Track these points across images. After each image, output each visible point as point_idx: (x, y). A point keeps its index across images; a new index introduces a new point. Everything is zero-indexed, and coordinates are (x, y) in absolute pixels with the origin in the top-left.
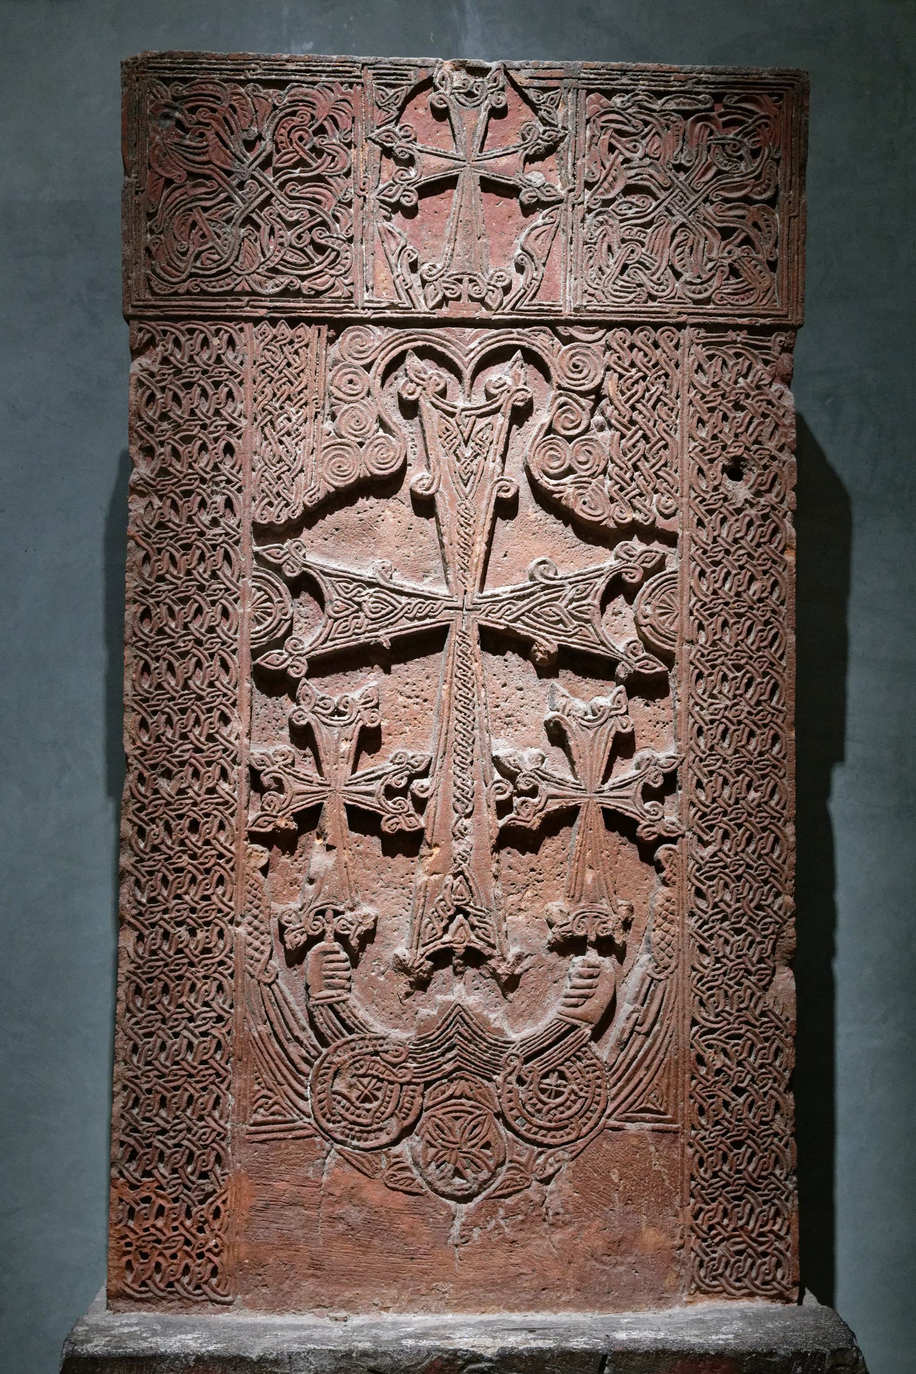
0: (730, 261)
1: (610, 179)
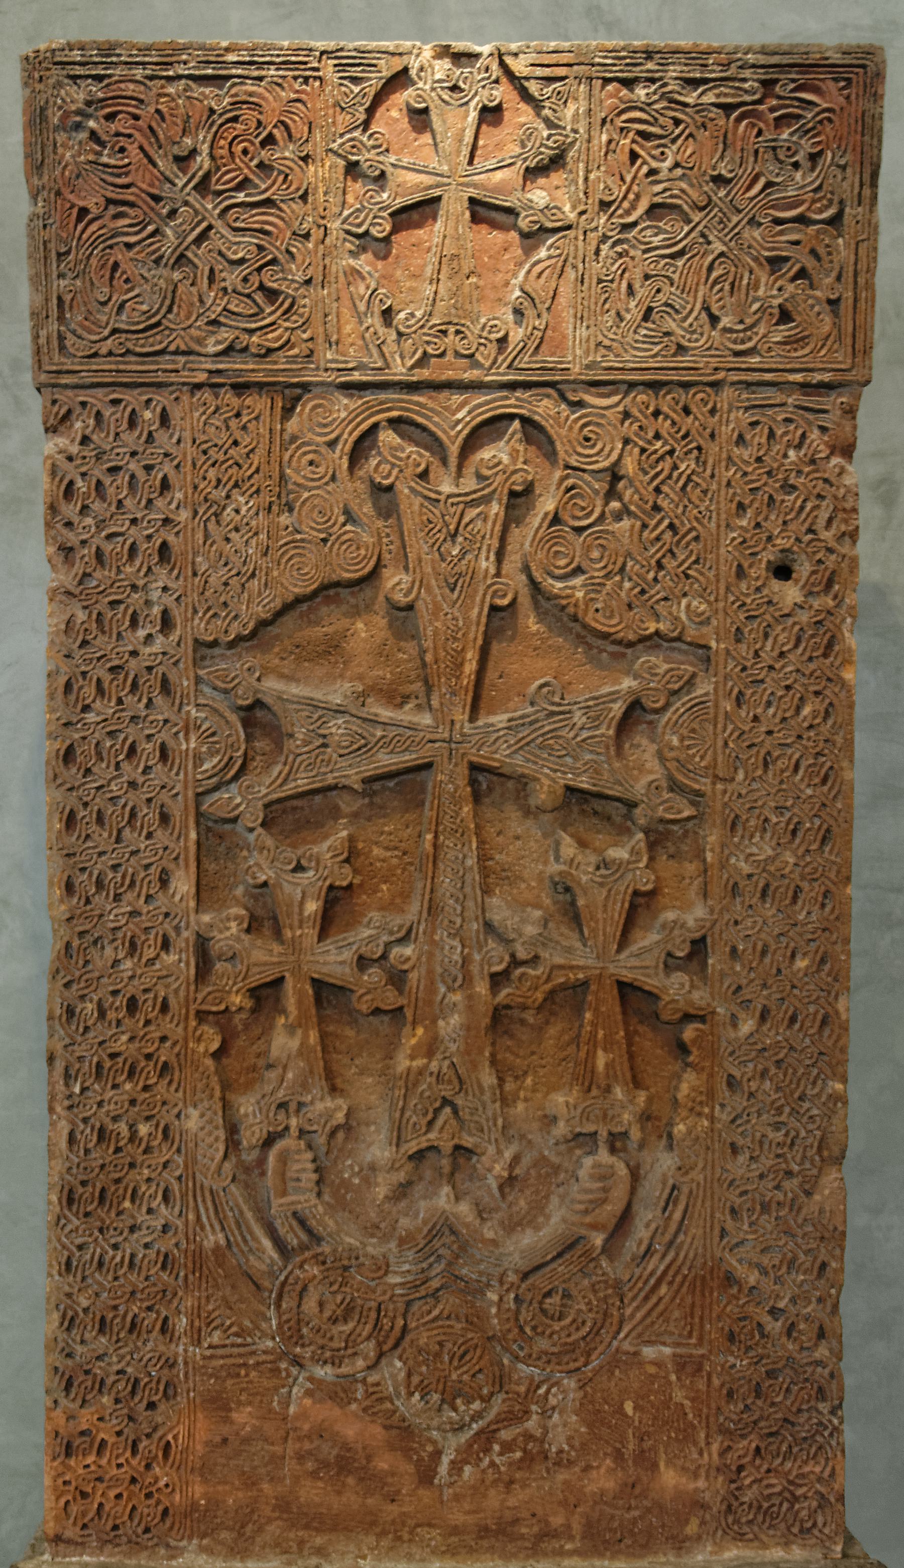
0: (780, 300)
1: (631, 196)
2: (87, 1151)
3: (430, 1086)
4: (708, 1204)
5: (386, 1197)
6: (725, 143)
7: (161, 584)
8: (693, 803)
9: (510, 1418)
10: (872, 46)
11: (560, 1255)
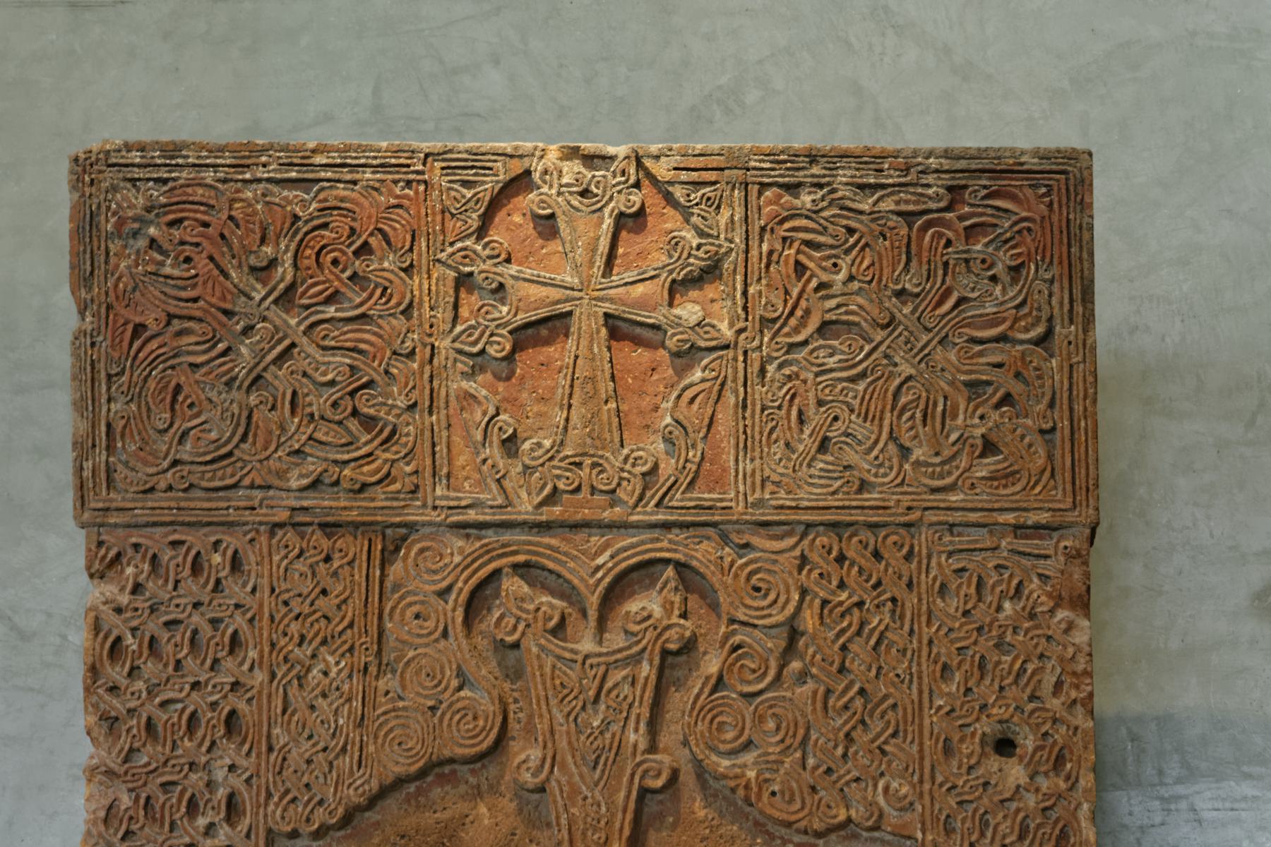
0: (983, 430)
1: (799, 313)
7: (228, 761)
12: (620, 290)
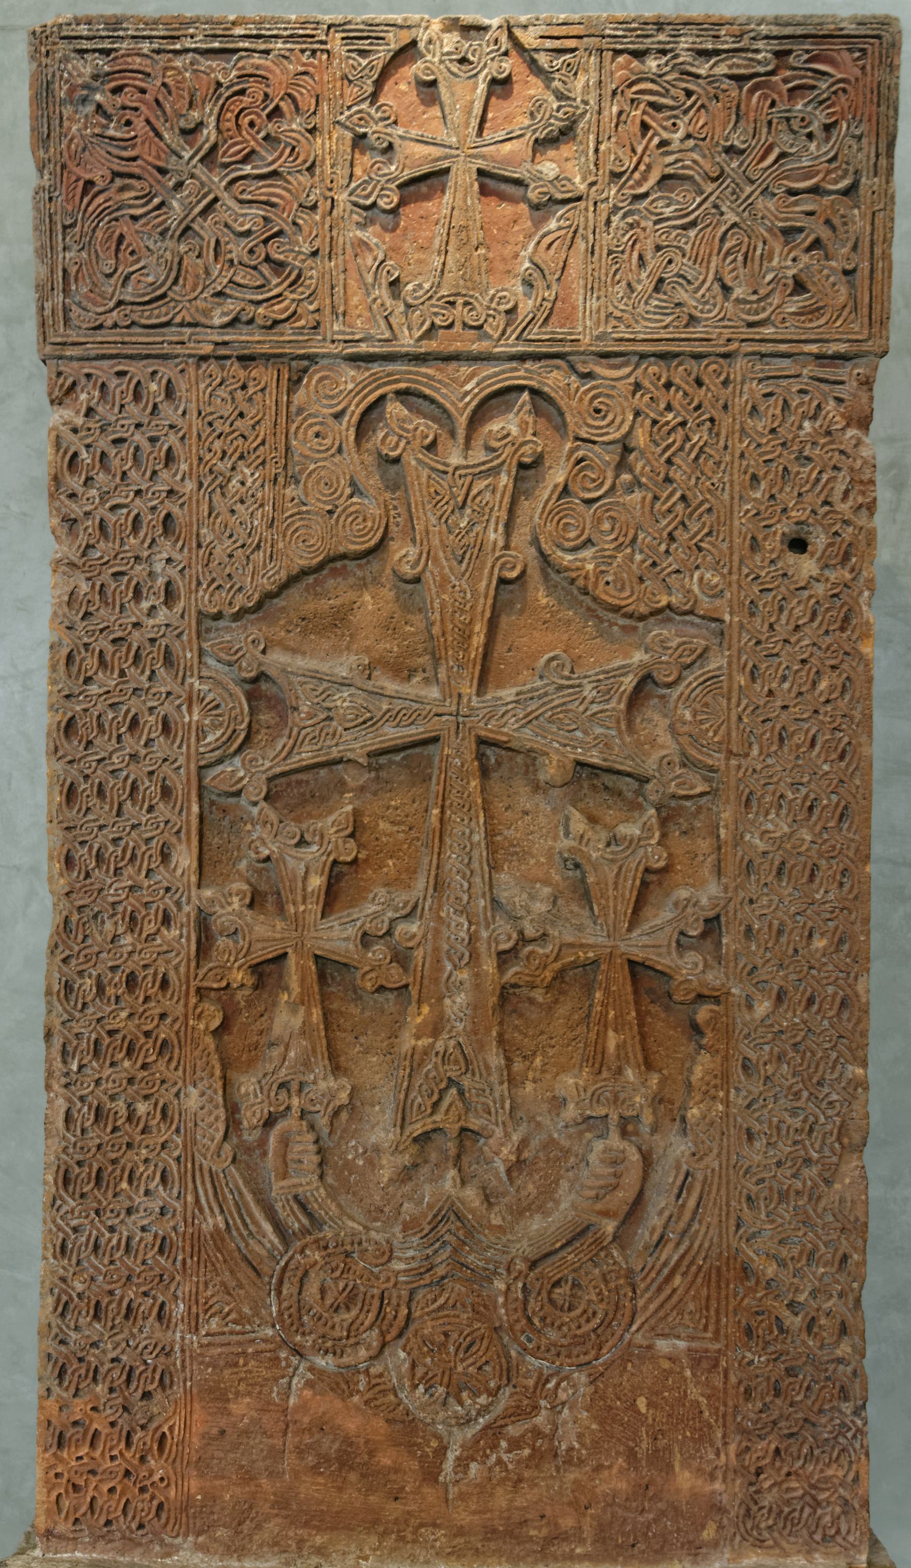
0: (794, 271)
1: (642, 167)
2: (83, 1131)
3: (436, 1067)
4: (723, 1192)
5: (390, 1180)
6: (738, 115)
7: (165, 555)
8: (706, 780)
9: (516, 1413)
10: (887, 17)
11: (569, 1243)
12: (492, 148)
